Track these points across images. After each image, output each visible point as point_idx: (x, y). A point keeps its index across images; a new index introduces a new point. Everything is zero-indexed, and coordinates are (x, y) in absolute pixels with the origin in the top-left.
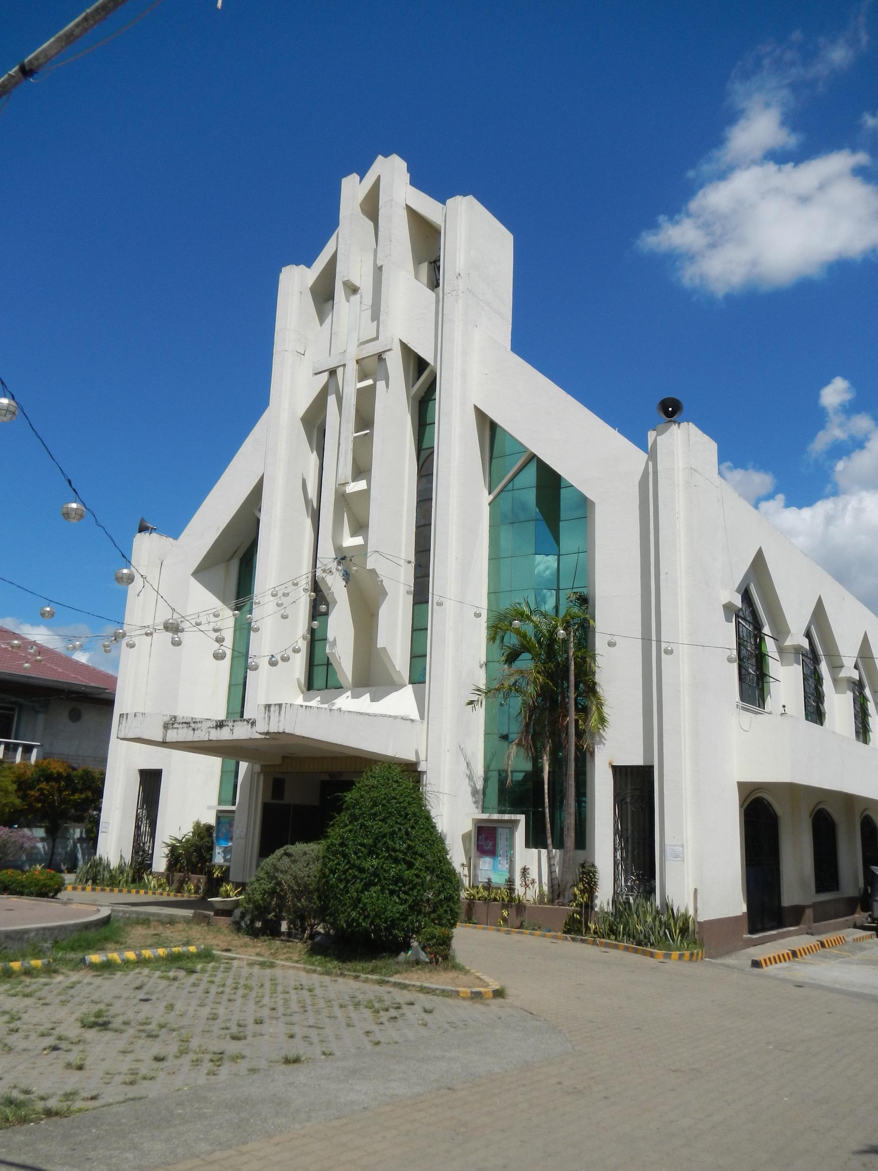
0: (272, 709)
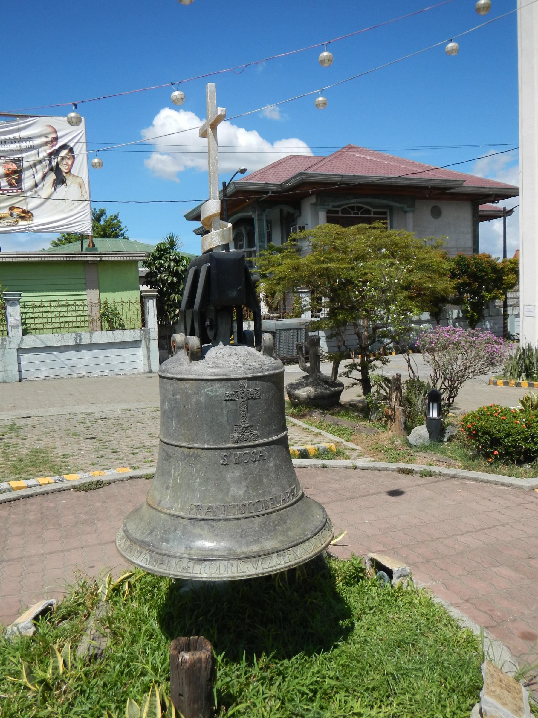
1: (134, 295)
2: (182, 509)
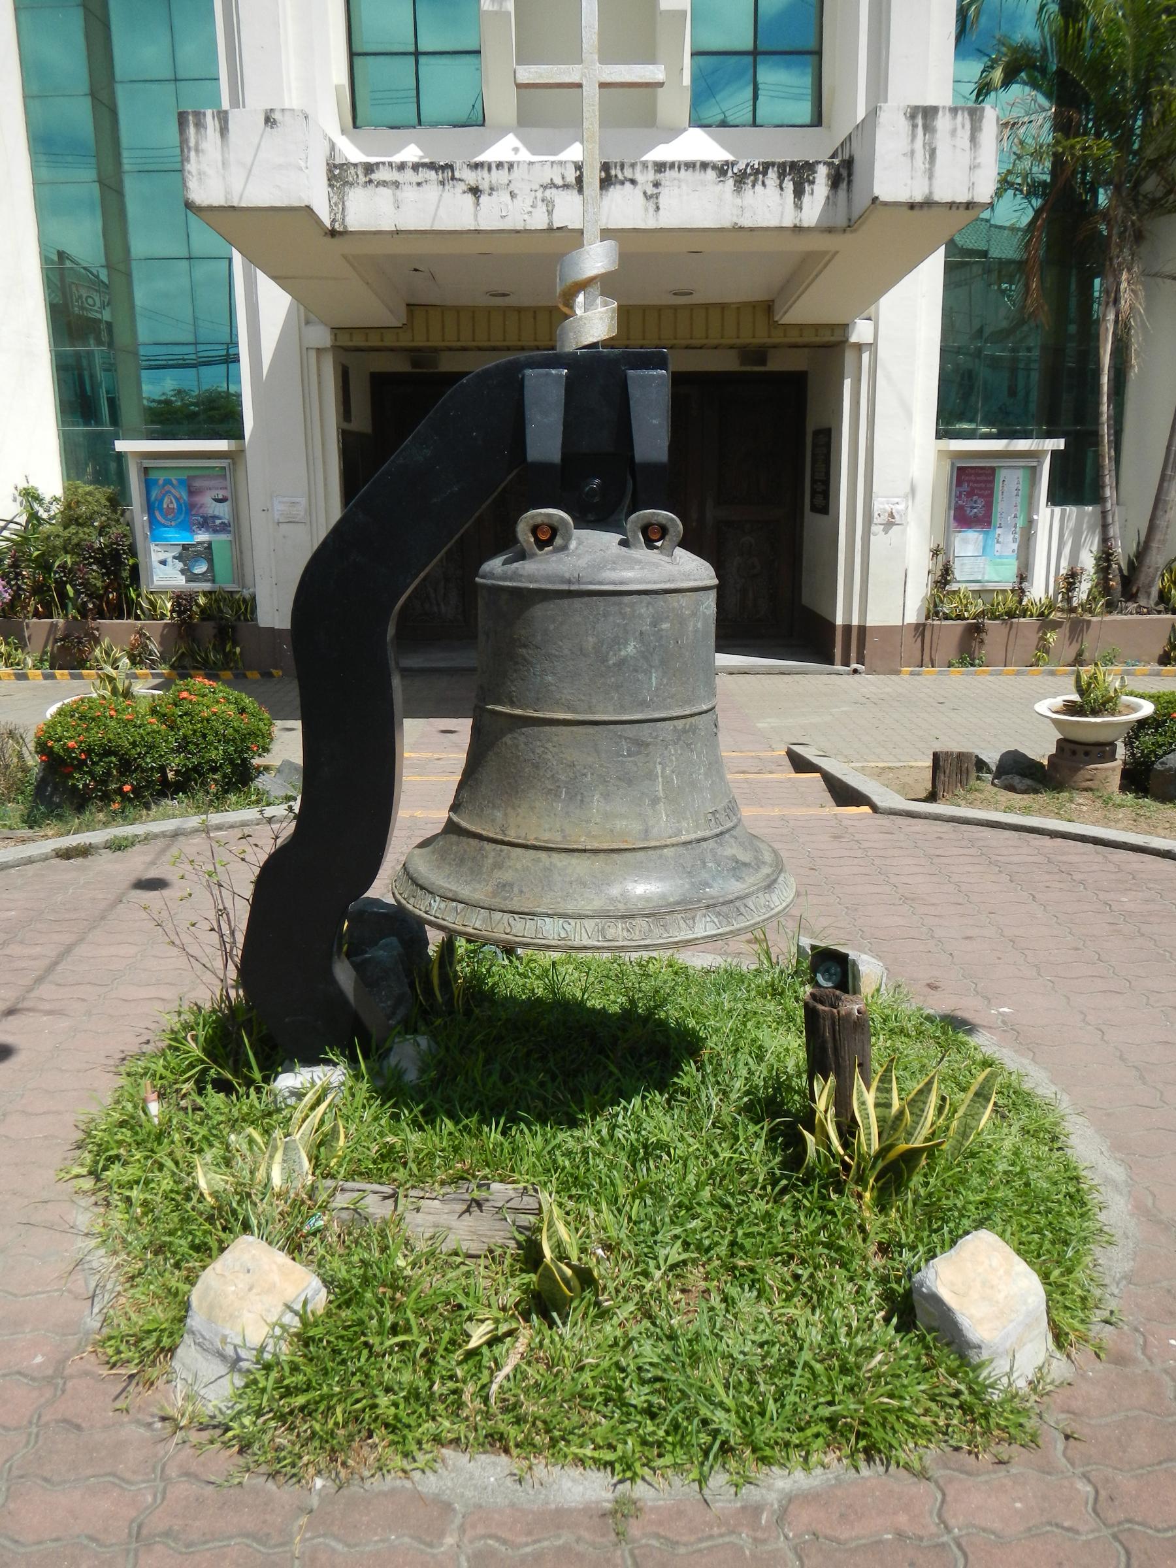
0: (943, 122)
2: (697, 827)
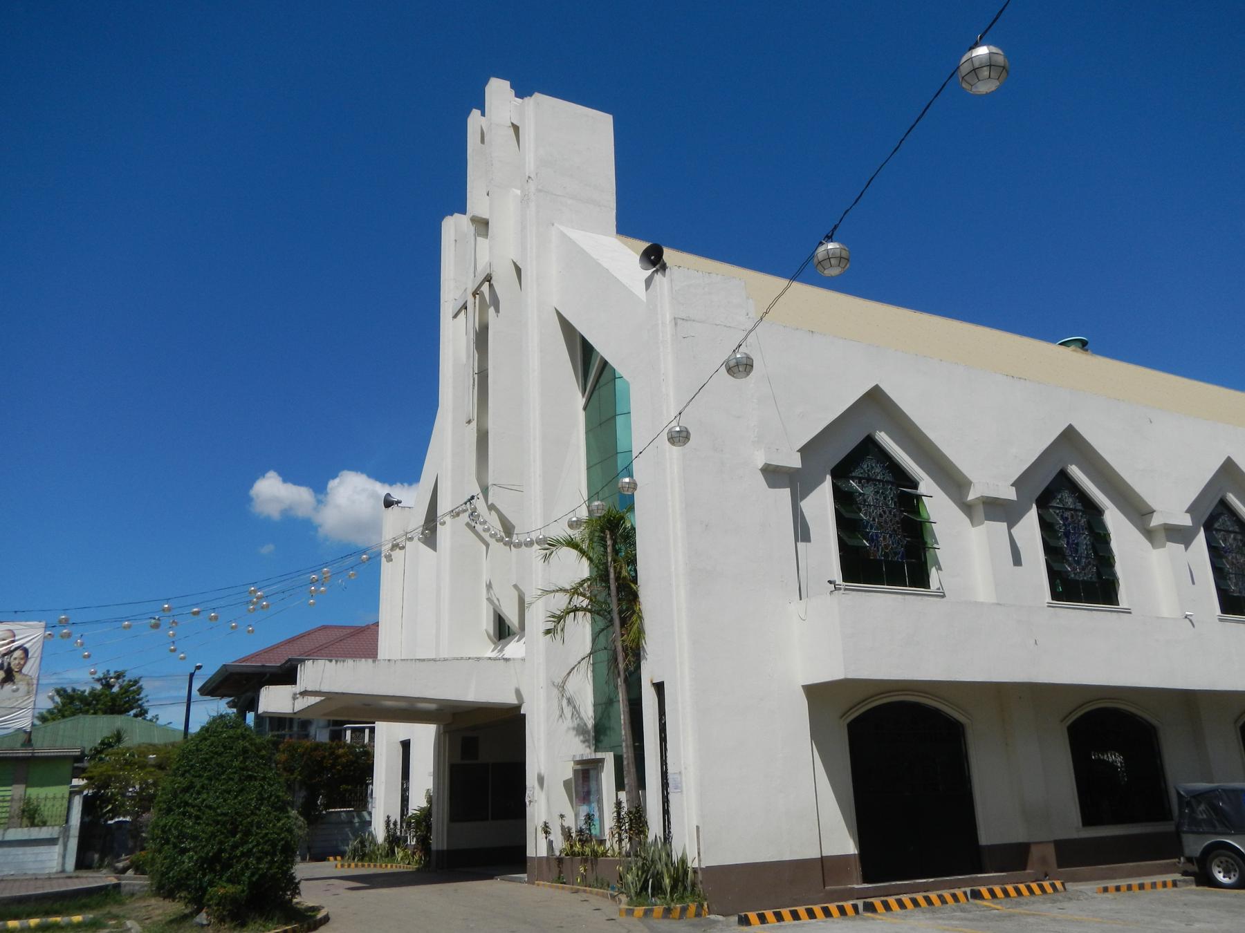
1: (64, 790)
